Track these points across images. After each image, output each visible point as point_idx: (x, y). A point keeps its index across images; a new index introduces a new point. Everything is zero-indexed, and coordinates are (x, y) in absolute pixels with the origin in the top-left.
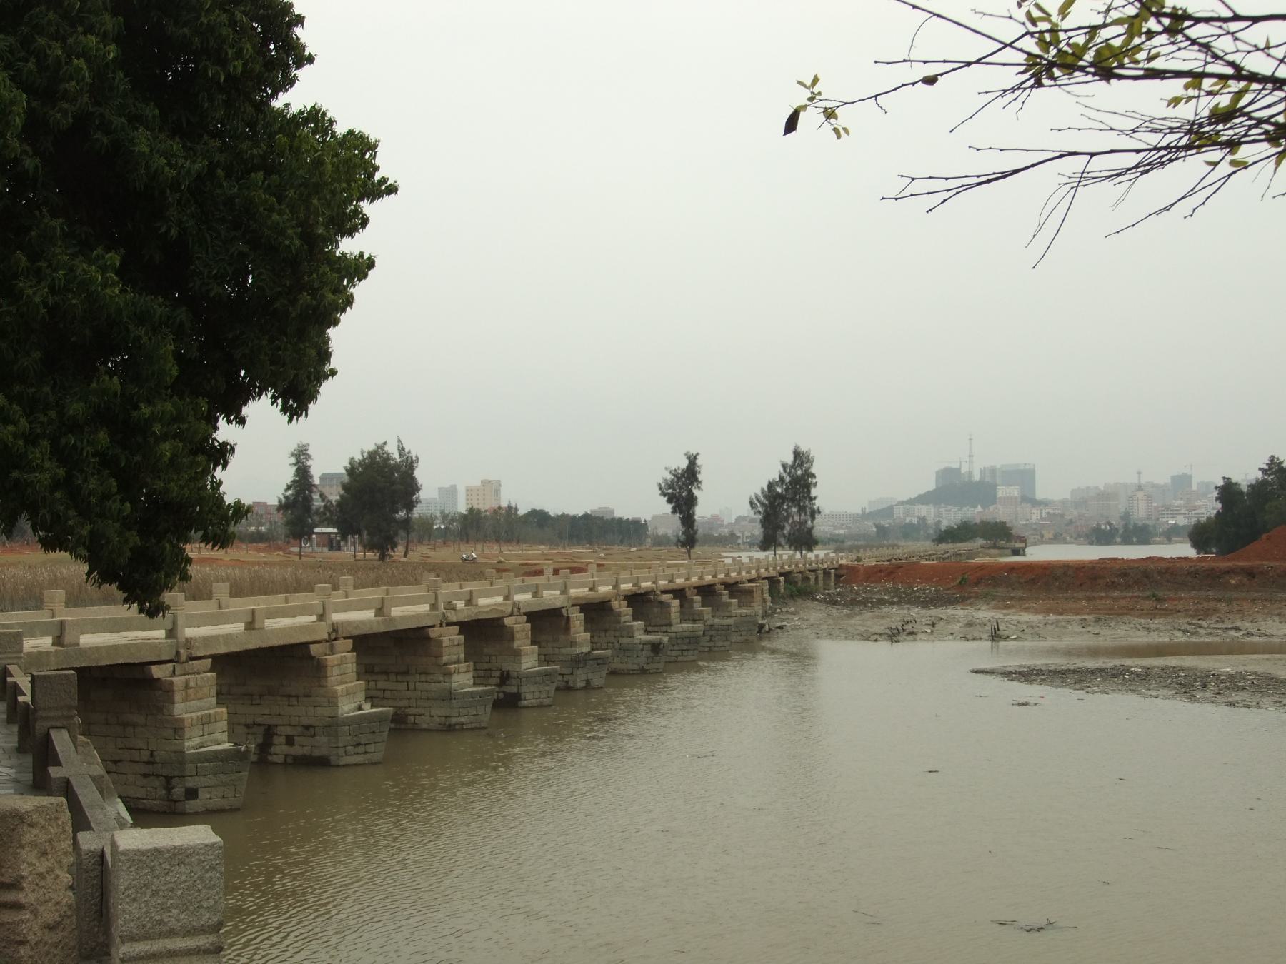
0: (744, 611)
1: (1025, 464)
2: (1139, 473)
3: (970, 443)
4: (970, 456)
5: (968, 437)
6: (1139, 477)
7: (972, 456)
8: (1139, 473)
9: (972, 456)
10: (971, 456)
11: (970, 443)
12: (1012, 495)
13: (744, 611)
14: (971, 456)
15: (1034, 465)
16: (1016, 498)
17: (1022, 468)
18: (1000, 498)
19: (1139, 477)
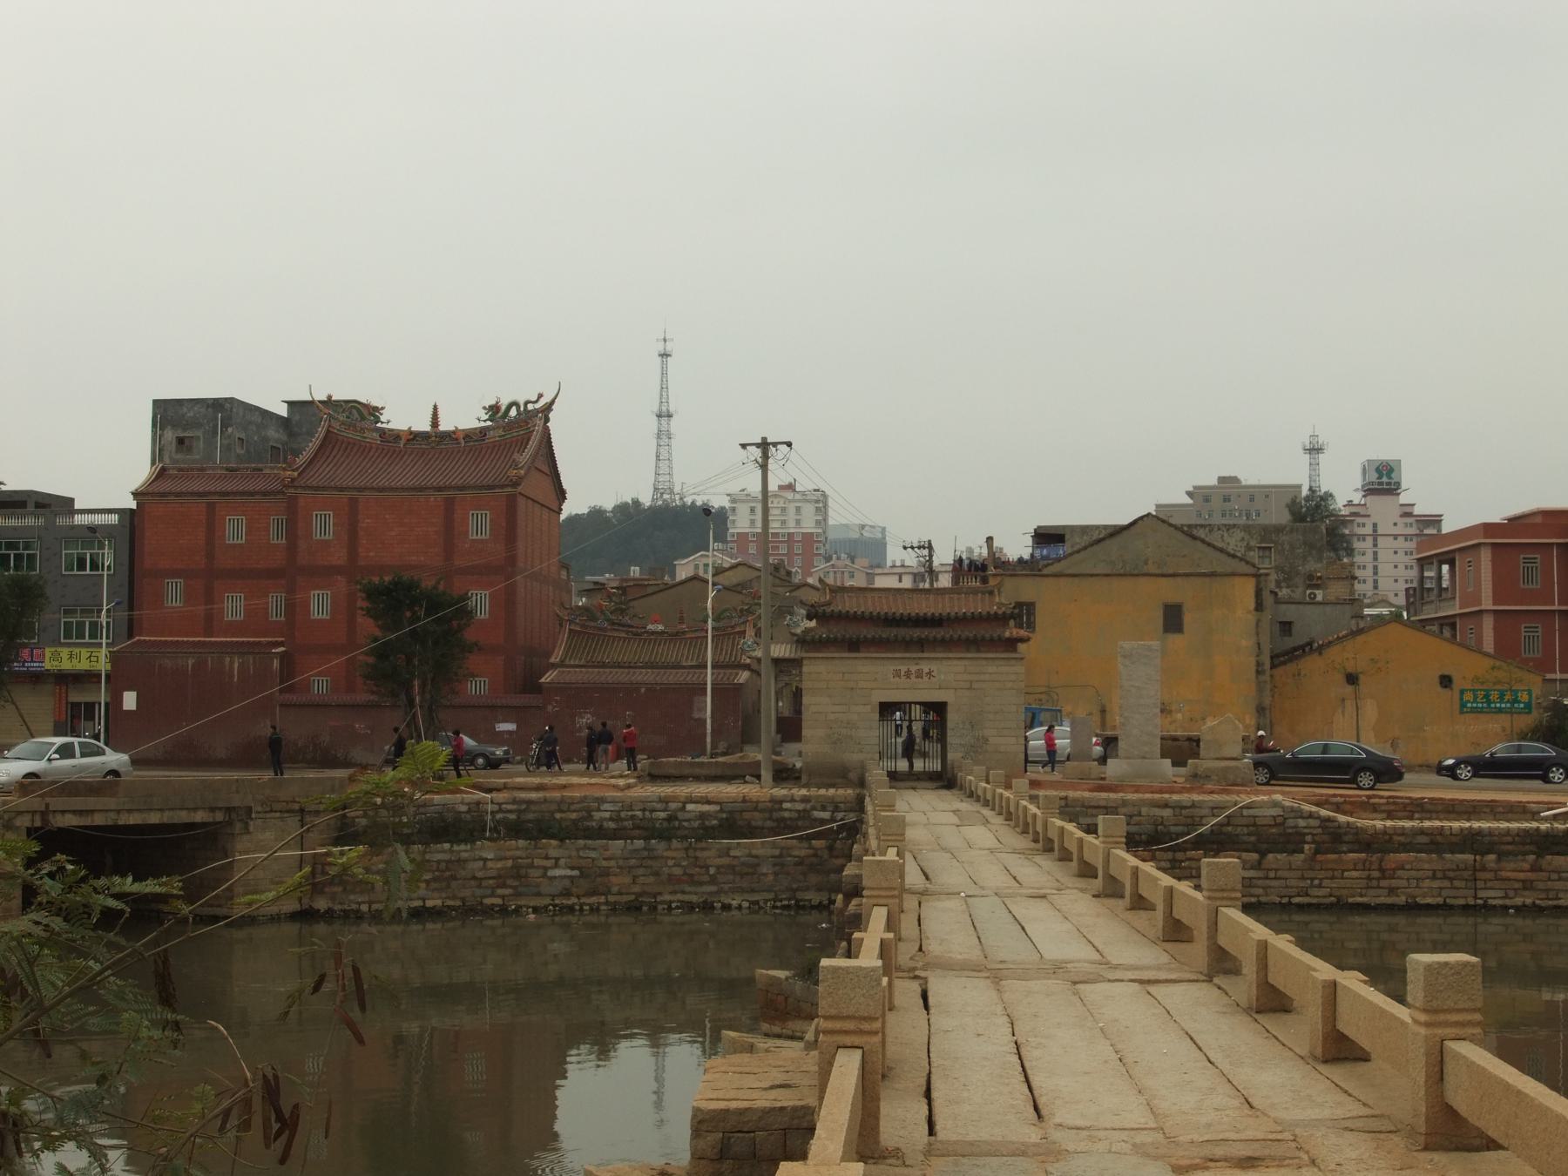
0: (150, 887)
1: (863, 527)
2: (1314, 450)
3: (664, 373)
4: (659, 416)
5: (660, 347)
6: (1314, 466)
7: (670, 416)
8: (1314, 450)
9: (670, 416)
10: (664, 415)
11: (664, 373)
12: (791, 528)
13: (150, 887)
14: (664, 415)
15: (884, 529)
16: (808, 538)
17: (855, 535)
18: (743, 537)
19: (1314, 466)
